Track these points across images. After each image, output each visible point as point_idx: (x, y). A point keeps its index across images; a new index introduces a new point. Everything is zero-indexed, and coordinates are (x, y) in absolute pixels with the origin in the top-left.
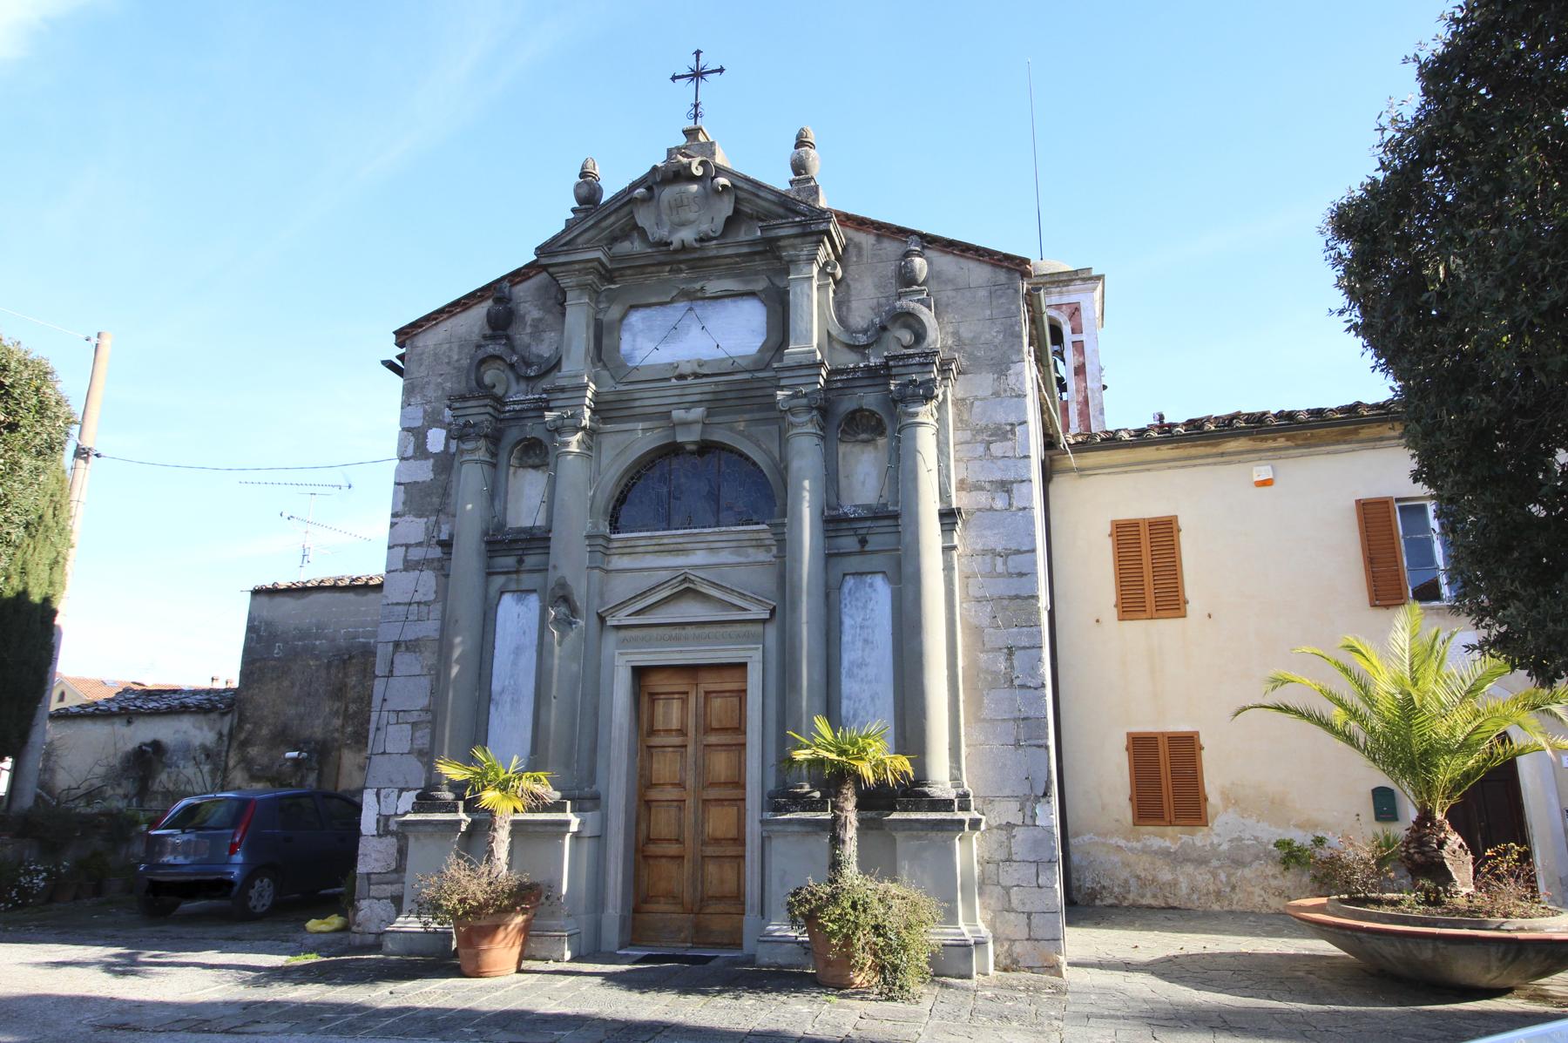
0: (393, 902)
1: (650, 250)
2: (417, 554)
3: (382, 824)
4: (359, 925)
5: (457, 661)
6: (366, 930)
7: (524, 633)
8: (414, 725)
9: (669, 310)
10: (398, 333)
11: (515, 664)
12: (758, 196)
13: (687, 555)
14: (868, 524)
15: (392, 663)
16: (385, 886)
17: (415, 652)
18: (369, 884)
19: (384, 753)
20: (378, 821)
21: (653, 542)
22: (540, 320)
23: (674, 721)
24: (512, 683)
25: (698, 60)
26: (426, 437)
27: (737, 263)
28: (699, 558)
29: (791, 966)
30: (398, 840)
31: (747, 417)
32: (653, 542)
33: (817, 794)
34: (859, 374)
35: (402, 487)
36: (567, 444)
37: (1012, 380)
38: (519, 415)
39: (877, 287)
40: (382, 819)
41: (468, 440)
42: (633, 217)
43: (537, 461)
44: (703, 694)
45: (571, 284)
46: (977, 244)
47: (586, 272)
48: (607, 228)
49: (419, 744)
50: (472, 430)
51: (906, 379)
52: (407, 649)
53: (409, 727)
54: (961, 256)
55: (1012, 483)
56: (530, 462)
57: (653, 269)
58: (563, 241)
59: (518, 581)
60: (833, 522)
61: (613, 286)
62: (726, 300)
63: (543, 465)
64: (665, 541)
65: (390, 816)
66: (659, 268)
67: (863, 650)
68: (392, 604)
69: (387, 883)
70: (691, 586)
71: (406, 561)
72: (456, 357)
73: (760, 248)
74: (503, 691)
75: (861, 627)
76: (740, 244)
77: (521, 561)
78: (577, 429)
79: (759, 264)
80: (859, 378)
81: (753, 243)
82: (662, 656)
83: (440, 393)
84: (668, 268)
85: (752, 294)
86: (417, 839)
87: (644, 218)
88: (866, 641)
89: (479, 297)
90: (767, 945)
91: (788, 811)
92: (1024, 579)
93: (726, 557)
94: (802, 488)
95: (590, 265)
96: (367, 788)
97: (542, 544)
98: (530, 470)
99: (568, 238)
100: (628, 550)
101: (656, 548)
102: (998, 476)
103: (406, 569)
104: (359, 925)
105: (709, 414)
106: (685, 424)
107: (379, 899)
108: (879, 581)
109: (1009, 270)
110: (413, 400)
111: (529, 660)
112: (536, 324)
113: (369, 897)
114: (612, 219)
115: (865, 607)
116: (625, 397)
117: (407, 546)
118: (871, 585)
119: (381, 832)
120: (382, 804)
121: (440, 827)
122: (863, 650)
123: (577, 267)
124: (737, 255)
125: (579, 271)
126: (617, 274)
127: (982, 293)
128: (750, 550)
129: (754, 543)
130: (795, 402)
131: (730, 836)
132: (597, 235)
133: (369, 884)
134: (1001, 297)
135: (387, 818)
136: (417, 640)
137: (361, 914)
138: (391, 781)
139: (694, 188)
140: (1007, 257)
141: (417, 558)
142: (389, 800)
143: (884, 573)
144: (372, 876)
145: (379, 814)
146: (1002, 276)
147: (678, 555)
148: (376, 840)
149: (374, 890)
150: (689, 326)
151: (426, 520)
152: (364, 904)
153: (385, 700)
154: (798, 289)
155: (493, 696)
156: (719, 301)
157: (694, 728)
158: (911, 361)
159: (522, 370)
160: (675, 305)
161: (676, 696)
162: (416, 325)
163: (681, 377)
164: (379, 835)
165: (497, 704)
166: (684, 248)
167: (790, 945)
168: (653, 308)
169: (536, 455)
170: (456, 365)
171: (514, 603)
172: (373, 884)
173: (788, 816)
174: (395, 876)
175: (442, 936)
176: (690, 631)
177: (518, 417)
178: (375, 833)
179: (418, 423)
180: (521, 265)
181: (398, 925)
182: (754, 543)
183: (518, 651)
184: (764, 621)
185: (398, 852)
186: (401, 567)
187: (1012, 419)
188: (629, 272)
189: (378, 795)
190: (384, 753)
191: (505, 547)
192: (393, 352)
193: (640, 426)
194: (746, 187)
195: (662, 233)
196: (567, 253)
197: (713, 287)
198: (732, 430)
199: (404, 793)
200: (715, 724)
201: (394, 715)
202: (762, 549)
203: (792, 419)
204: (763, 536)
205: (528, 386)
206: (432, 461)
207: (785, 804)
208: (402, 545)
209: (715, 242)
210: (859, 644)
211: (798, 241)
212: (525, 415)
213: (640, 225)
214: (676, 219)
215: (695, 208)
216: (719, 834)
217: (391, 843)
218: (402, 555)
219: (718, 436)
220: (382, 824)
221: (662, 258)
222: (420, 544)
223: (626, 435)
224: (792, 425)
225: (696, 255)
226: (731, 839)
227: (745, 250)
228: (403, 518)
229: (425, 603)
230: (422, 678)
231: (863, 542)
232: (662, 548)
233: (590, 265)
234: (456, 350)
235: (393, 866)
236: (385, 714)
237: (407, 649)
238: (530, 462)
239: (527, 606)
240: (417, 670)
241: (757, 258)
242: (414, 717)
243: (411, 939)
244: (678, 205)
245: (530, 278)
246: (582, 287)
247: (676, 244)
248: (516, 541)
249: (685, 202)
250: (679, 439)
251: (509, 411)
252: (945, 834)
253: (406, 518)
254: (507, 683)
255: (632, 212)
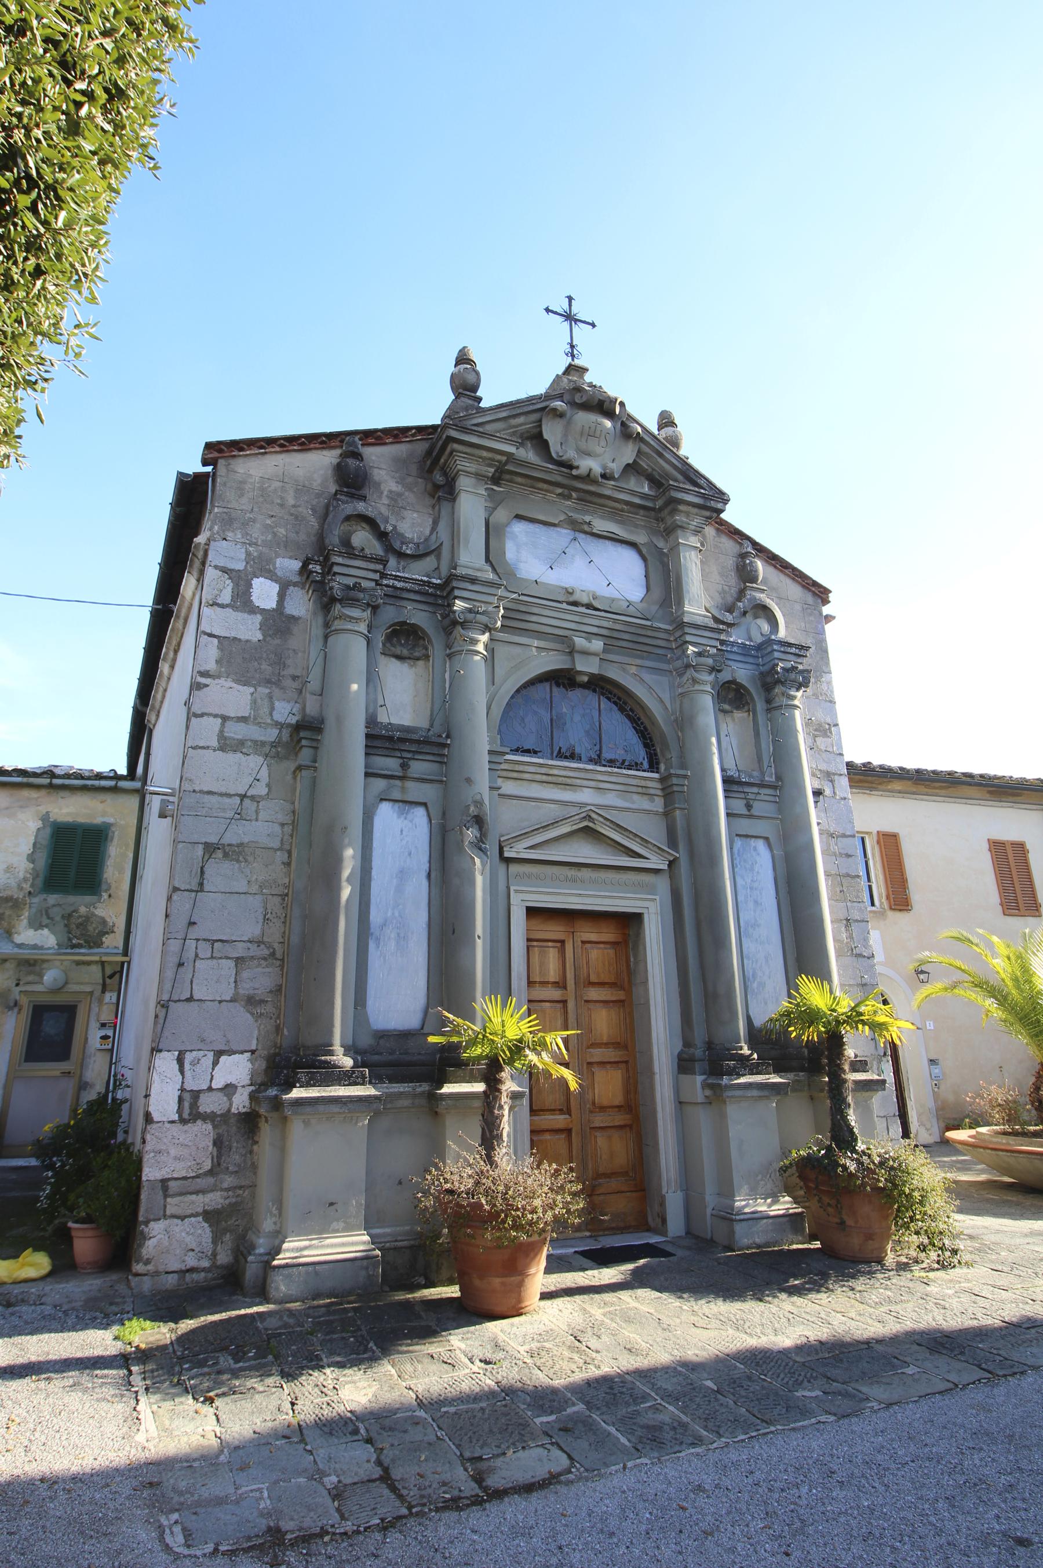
0: (206, 1220)
1: (551, 466)
2: (237, 732)
3: (186, 1105)
4: (148, 1262)
5: (348, 880)
6: (161, 1268)
7: (410, 854)
8: (239, 961)
9: (552, 532)
10: (209, 446)
11: (399, 889)
12: (661, 455)
13: (575, 791)
14: (755, 790)
15: (202, 872)
16: (194, 1197)
17: (238, 861)
18: (166, 1196)
19: (190, 999)
20: (180, 1099)
21: (544, 770)
22: (400, 495)
23: (552, 973)
24: (397, 914)
25: (570, 305)
26: (250, 586)
27: (622, 510)
28: (586, 796)
29: (768, 1244)
30: (215, 1127)
31: (639, 662)
32: (544, 770)
33: (755, 1056)
34: (735, 649)
35: (216, 641)
36: (475, 642)
37: (824, 687)
38: (398, 593)
39: (721, 575)
40: (187, 1096)
41: (351, 606)
42: (540, 426)
43: (405, 652)
44: (580, 943)
45: (468, 469)
46: (796, 565)
47: (489, 462)
48: (514, 427)
49: (246, 988)
50: (361, 595)
51: (789, 665)
52: (226, 855)
53: (231, 963)
54: (781, 571)
55: (834, 774)
56: (398, 650)
57: (545, 486)
58: (475, 421)
59: (403, 789)
60: (727, 781)
61: (495, 488)
62: (607, 542)
63: (409, 658)
64: (555, 772)
65: (199, 1092)
66: (551, 488)
67: (755, 911)
68: (201, 792)
69: (197, 1192)
70: (591, 825)
71: (221, 736)
72: (291, 501)
73: (650, 504)
74: (384, 925)
75: (751, 888)
76: (633, 493)
77: (404, 766)
78: (487, 628)
79: (640, 518)
80: (735, 652)
81: (644, 496)
82: (560, 898)
83: (270, 537)
84: (559, 491)
85: (633, 545)
86: (307, 1123)
87: (551, 432)
88: (756, 902)
89: (323, 442)
90: (744, 1224)
91: (739, 1075)
92: (850, 859)
93: (611, 799)
94: (711, 743)
95: (499, 457)
96: (161, 1051)
97: (435, 750)
98: (393, 660)
99: (480, 420)
100: (515, 775)
101: (544, 778)
102: (823, 767)
103: (222, 748)
104: (148, 1262)
105: (604, 651)
106: (585, 653)
107: (182, 1218)
108: (760, 844)
109: (814, 594)
110: (230, 535)
111: (418, 888)
112: (394, 497)
113: (165, 1216)
114: (521, 420)
115: (752, 869)
116: (523, 608)
117: (225, 719)
118: (755, 849)
119: (186, 1116)
120: (188, 1074)
121: (350, 1106)
122: (755, 911)
123: (485, 454)
124: (627, 503)
125: (484, 459)
126: (508, 477)
127: (798, 607)
128: (635, 797)
129: (640, 790)
130: (702, 660)
131: (617, 1103)
132: (504, 430)
133: (166, 1196)
134: (810, 615)
135: (196, 1094)
136: (241, 845)
137: (150, 1244)
138: (203, 1041)
139: (608, 424)
140: (815, 584)
141: (240, 737)
142: (198, 1068)
143: (766, 839)
144: (171, 1184)
145: (182, 1090)
146: (810, 598)
147: (565, 789)
148: (179, 1126)
149: (174, 1205)
150: (573, 556)
151: (252, 690)
152: (156, 1229)
153: (192, 924)
154: (687, 554)
155: (372, 930)
156: (601, 541)
157: (573, 982)
158: (789, 650)
159: (397, 545)
160: (558, 529)
161: (550, 944)
162: (237, 446)
163: (575, 604)
164: (183, 1121)
165: (378, 939)
166: (588, 478)
167: (765, 1221)
168: (537, 525)
169: (402, 645)
170: (293, 510)
171: (395, 816)
172: (173, 1196)
173: (742, 1080)
174: (211, 1180)
175: (365, 1262)
176: (586, 873)
177: (395, 596)
178: (176, 1117)
179: (240, 566)
180: (380, 426)
181: (288, 1255)
182: (640, 790)
183: (402, 874)
184: (657, 871)
185: (215, 1144)
186: (215, 743)
187: (829, 720)
188: (519, 480)
189: (180, 1061)
190: (190, 999)
191: (387, 745)
192: (194, 466)
193: (536, 643)
194: (652, 442)
195: (570, 454)
196: (482, 435)
197: (601, 525)
198: (624, 670)
199: (223, 1059)
200: (593, 978)
201: (208, 945)
202: (646, 797)
203: (695, 675)
204: (650, 784)
205: (399, 563)
206: (259, 618)
207: (735, 1067)
208: (216, 716)
209: (612, 483)
210: (751, 905)
211: (695, 510)
212: (405, 595)
213: (546, 436)
214: (583, 445)
215: (603, 443)
216: (605, 1103)
217: (202, 1134)
218: (217, 729)
219: (613, 673)
220: (186, 1105)
221: (559, 479)
222: (243, 719)
223: (518, 650)
224: (695, 681)
225: (592, 488)
226: (618, 1107)
227: (637, 501)
228: (217, 681)
229: (253, 798)
230: (251, 898)
231: (749, 807)
232: (550, 779)
233: (499, 457)
234: (292, 493)
235: (207, 1165)
236: (191, 944)
237: (226, 855)
238: (398, 650)
239: (411, 821)
240: (241, 886)
241: (642, 512)
242: (239, 951)
243: (316, 1273)
244: (591, 434)
245: (385, 444)
246: (479, 476)
247: (582, 471)
248: (402, 740)
249: (598, 434)
250: (579, 668)
251: (387, 586)
252: (866, 1094)
253: (222, 681)
254: (389, 914)
255: (540, 421)
